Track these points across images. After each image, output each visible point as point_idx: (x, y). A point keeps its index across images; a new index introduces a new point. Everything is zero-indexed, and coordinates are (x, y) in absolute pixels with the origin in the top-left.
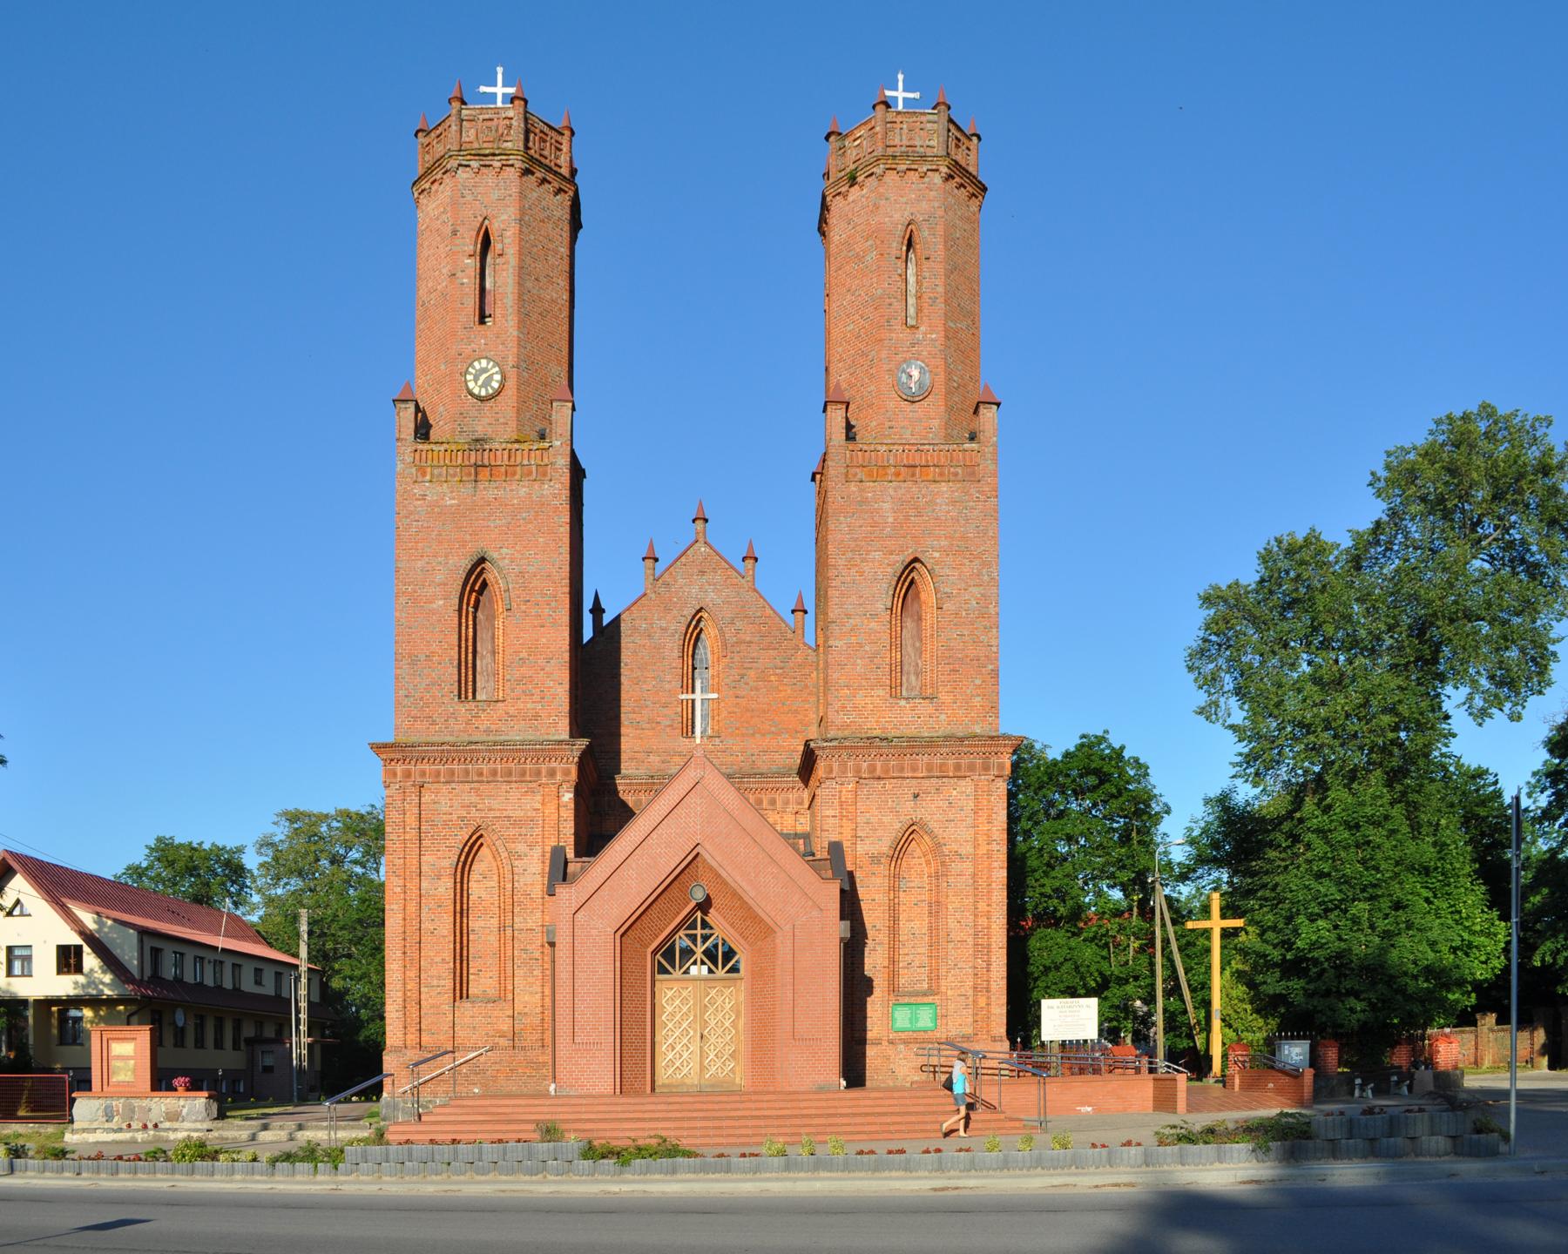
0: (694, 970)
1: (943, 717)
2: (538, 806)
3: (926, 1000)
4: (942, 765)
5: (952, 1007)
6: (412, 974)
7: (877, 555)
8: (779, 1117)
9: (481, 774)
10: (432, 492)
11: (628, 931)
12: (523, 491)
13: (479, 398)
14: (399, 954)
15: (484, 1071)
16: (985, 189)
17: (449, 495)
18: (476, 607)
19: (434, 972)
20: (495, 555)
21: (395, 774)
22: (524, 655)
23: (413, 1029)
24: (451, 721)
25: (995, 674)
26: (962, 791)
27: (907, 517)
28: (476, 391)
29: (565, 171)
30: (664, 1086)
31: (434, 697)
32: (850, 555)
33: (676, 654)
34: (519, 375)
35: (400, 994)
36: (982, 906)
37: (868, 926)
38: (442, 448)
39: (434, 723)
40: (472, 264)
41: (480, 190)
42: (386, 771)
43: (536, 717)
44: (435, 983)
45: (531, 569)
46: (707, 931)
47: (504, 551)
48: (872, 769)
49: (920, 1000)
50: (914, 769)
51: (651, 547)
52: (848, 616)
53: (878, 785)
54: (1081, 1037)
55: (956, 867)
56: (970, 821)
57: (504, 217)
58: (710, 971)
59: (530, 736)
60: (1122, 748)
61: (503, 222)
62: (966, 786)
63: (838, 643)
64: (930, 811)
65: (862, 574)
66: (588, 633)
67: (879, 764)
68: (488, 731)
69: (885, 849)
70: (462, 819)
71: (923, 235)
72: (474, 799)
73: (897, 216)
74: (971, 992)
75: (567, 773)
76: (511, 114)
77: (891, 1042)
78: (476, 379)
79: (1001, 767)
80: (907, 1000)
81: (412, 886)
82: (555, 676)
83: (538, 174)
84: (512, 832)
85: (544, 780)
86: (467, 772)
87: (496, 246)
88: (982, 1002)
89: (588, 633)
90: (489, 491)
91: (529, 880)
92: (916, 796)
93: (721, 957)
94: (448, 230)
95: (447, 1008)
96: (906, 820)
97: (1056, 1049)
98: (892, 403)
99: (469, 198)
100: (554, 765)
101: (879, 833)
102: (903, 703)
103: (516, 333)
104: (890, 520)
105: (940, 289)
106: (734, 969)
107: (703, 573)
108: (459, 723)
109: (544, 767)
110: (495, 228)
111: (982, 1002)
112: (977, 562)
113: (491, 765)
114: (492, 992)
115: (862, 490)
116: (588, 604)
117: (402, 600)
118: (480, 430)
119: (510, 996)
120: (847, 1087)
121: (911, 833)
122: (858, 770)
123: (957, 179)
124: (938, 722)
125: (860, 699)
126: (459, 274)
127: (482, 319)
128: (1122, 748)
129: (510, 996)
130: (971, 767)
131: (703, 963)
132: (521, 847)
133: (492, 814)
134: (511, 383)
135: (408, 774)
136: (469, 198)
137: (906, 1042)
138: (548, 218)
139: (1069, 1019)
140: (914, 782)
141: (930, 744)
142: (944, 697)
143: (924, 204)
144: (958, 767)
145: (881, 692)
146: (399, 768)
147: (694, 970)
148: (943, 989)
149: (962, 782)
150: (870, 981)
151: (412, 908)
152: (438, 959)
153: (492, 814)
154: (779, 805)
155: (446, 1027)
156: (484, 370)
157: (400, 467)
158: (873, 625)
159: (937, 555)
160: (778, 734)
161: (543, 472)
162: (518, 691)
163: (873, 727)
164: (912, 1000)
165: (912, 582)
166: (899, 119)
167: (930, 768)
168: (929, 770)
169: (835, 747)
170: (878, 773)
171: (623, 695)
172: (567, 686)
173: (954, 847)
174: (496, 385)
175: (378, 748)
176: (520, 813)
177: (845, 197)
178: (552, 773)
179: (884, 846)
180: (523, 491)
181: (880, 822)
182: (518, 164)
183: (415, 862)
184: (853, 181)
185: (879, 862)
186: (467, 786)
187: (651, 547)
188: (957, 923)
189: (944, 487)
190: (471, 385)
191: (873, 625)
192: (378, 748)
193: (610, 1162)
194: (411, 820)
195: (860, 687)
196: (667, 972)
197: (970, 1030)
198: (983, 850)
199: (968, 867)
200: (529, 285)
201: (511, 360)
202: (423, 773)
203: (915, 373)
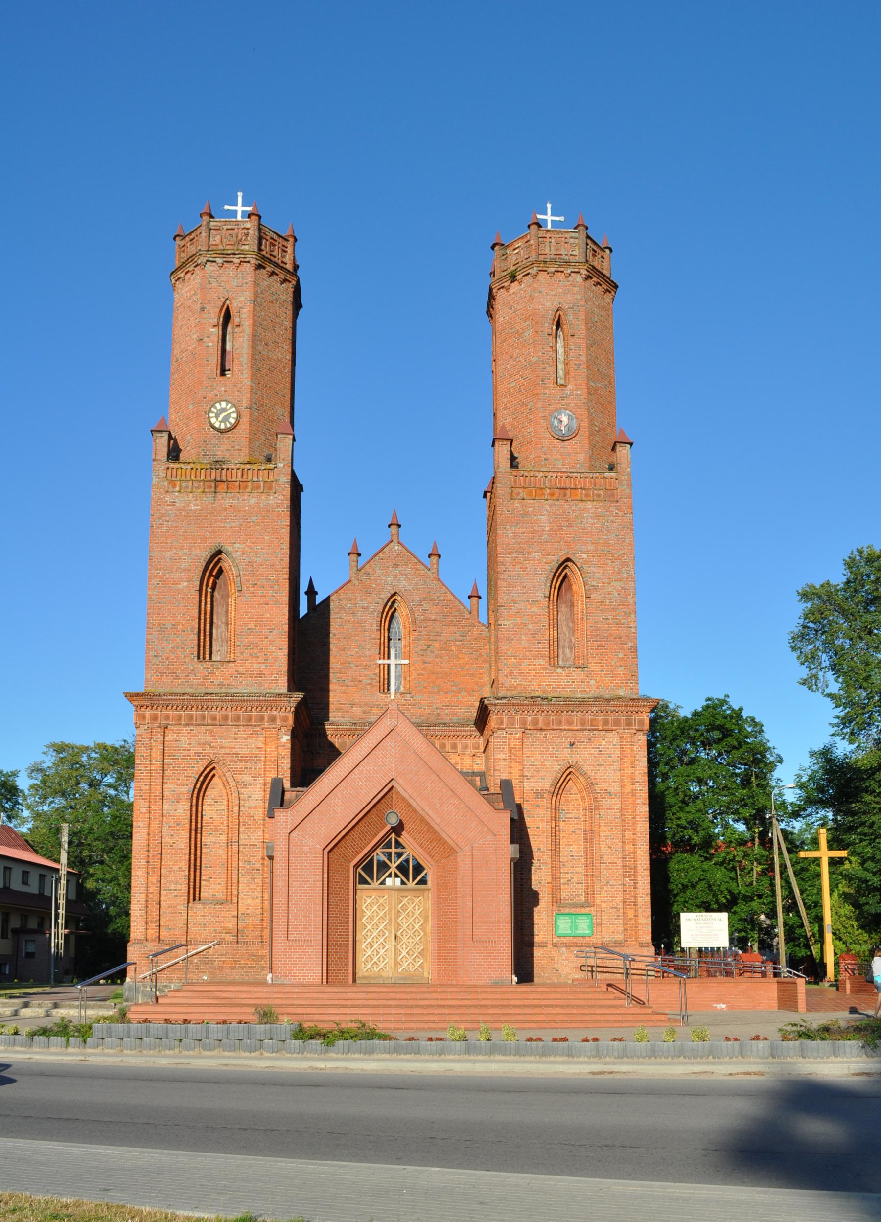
0: (389, 882)
1: (593, 682)
2: (261, 745)
3: (583, 911)
4: (592, 720)
5: (605, 917)
6: (154, 879)
7: (537, 555)
8: (461, 1006)
9: (215, 719)
10: (180, 500)
11: (333, 848)
12: (253, 501)
13: (219, 430)
14: (143, 862)
15: (212, 962)
16: (616, 287)
17: (195, 502)
18: (214, 588)
19: (172, 878)
20: (230, 549)
21: (144, 718)
22: (251, 626)
23: (153, 925)
24: (192, 677)
25: (634, 650)
26: (610, 741)
27: (560, 527)
28: (217, 425)
29: (289, 267)
30: (364, 978)
31: (178, 657)
32: (515, 555)
33: (375, 627)
34: (251, 415)
35: (143, 896)
36: (628, 834)
37: (534, 848)
38: (189, 467)
39: (177, 678)
40: (216, 332)
41: (223, 279)
42: (137, 715)
43: (261, 675)
44: (173, 887)
45: (259, 560)
46: (399, 850)
47: (237, 545)
48: (535, 722)
49: (578, 910)
50: (570, 723)
51: (355, 545)
53: (540, 735)
54: (715, 945)
55: (606, 802)
56: (616, 765)
57: (242, 299)
58: (403, 883)
59: (255, 689)
60: (741, 709)
61: (241, 302)
62: (613, 738)
63: (507, 623)
64: (584, 757)
65: (524, 569)
66: (303, 610)
67: (541, 719)
68: (221, 685)
69: (547, 787)
70: (198, 754)
71: (569, 319)
72: (209, 738)
73: (548, 304)
74: (621, 906)
75: (285, 719)
76: (248, 225)
77: (555, 945)
78: (217, 417)
79: (641, 722)
80: (567, 910)
81: (156, 807)
82: (276, 643)
83: (269, 269)
84: (240, 765)
85: (266, 725)
86: (203, 717)
87: (235, 319)
88: (631, 914)
89: (303, 610)
90: (226, 500)
91: (253, 805)
92: (572, 745)
93: (412, 871)
94: (198, 307)
95: (182, 908)
96: (564, 763)
97: (694, 955)
98: (547, 441)
99: (215, 284)
100: (274, 713)
101: (542, 773)
102: (559, 670)
103: (249, 383)
104: (547, 529)
105: (583, 358)
106: (423, 882)
107: (396, 565)
108: (195, 677)
109: (266, 715)
110: (234, 307)
111: (631, 914)
112: (617, 562)
113: (223, 712)
114: (220, 896)
115: (523, 506)
116: (304, 587)
117: (154, 581)
118: (220, 454)
119: (235, 899)
120: (518, 983)
121: (568, 774)
122: (524, 723)
123: (595, 279)
124: (588, 686)
125: (525, 666)
126: (206, 339)
127: (223, 372)
128: (741, 709)
129: (235, 899)
130: (617, 723)
131: (396, 876)
132: (246, 778)
133: (223, 751)
134: (245, 420)
135: (155, 718)
136: (215, 284)
137: (568, 946)
138: (276, 300)
139: (704, 930)
140: (570, 733)
141: (583, 703)
142: (593, 666)
144: (606, 722)
145: (542, 662)
146: (148, 713)
147: (389, 882)
148: (598, 902)
149: (610, 735)
150: (536, 894)
151: (155, 825)
152: (176, 868)
153: (223, 751)
154: (459, 748)
155: (181, 924)
156: (224, 410)
157: (155, 480)
158: (534, 609)
159: (585, 556)
160: (459, 692)
161: (269, 487)
162: (247, 653)
163: (536, 688)
164: (572, 910)
165: (565, 576)
166: (548, 235)
167: (583, 722)
168: (582, 724)
169: (505, 704)
170: (541, 725)
171: (332, 659)
172: (286, 651)
173: (604, 786)
174: (233, 421)
175: (131, 696)
176: (245, 751)
177: (507, 289)
178: (273, 719)
179: (546, 784)
180: (253, 501)
181: (543, 765)
182: (253, 261)
183: (159, 788)
184: (513, 278)
185: (542, 797)
186: (203, 728)
187: (355, 545)
188: (608, 847)
189: (589, 505)
190: (213, 420)
191: (534, 609)
192: (131, 696)
193: (317, 1043)
194: (157, 755)
196: (367, 883)
197: (621, 937)
198: (628, 789)
199: (616, 802)
200: (260, 348)
201: (245, 403)
202: (167, 717)
203: (565, 419)
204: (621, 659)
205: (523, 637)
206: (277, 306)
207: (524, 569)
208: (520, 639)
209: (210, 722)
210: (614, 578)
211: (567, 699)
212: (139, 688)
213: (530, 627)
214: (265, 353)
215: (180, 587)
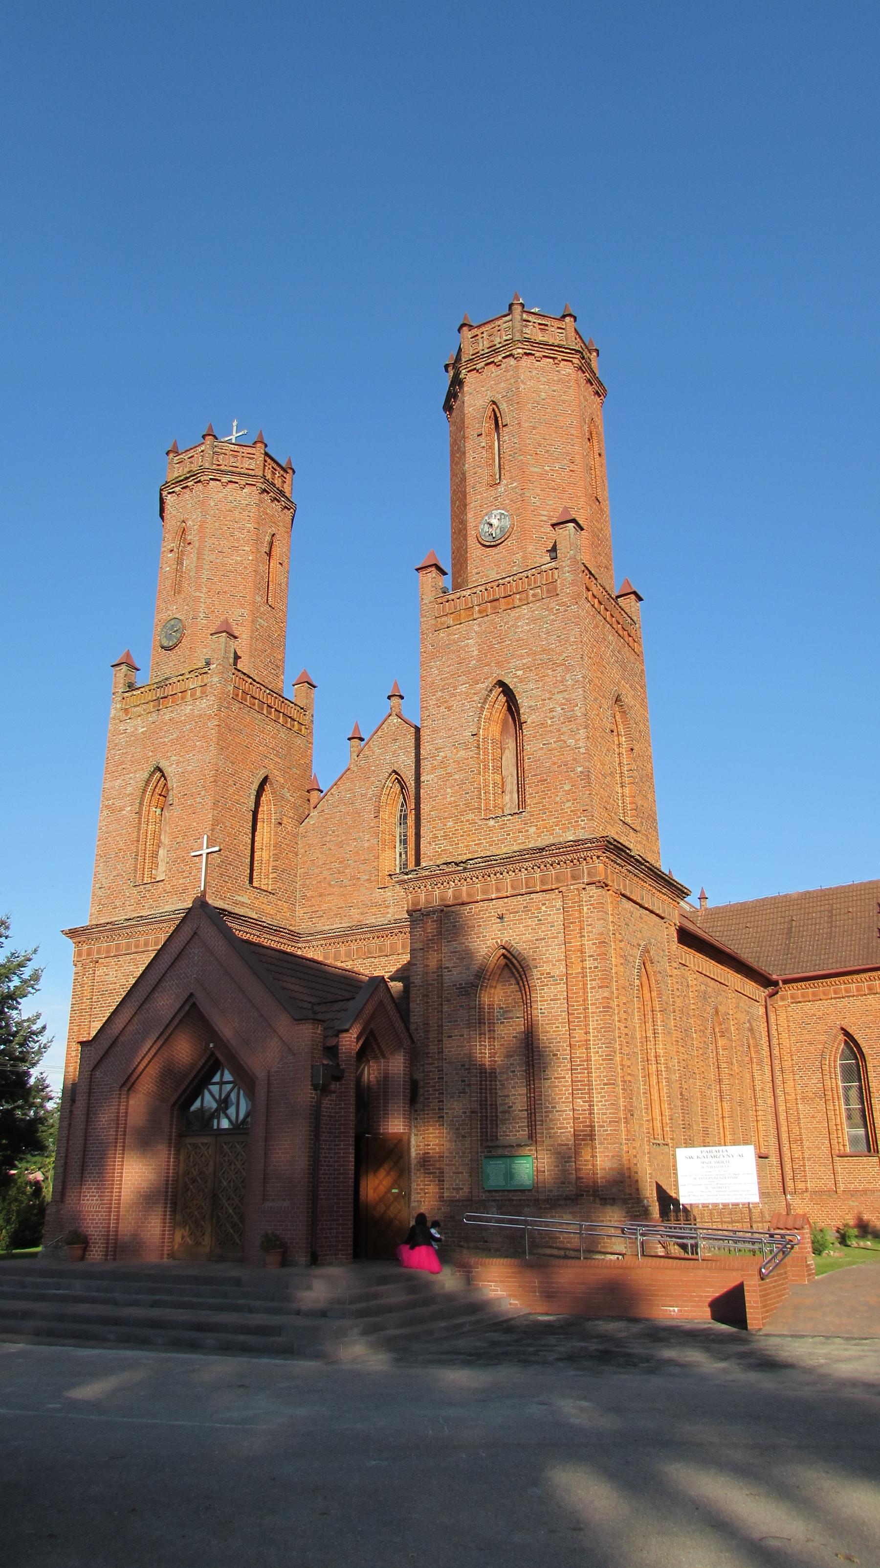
1: (533, 830)
63: (429, 777)
83: (224, 480)
92: (501, 918)
135: (89, 953)
140: (500, 902)
143: (503, 385)
146: (85, 947)
157: (113, 712)
159: (520, 673)
175: (72, 933)
189: (525, 610)
192: (72, 933)
198: (576, 969)
204: (567, 793)
206: (237, 513)
207: (449, 708)
210: (557, 690)
211: (486, 859)
212: (84, 922)
213: (457, 777)
214: (218, 561)
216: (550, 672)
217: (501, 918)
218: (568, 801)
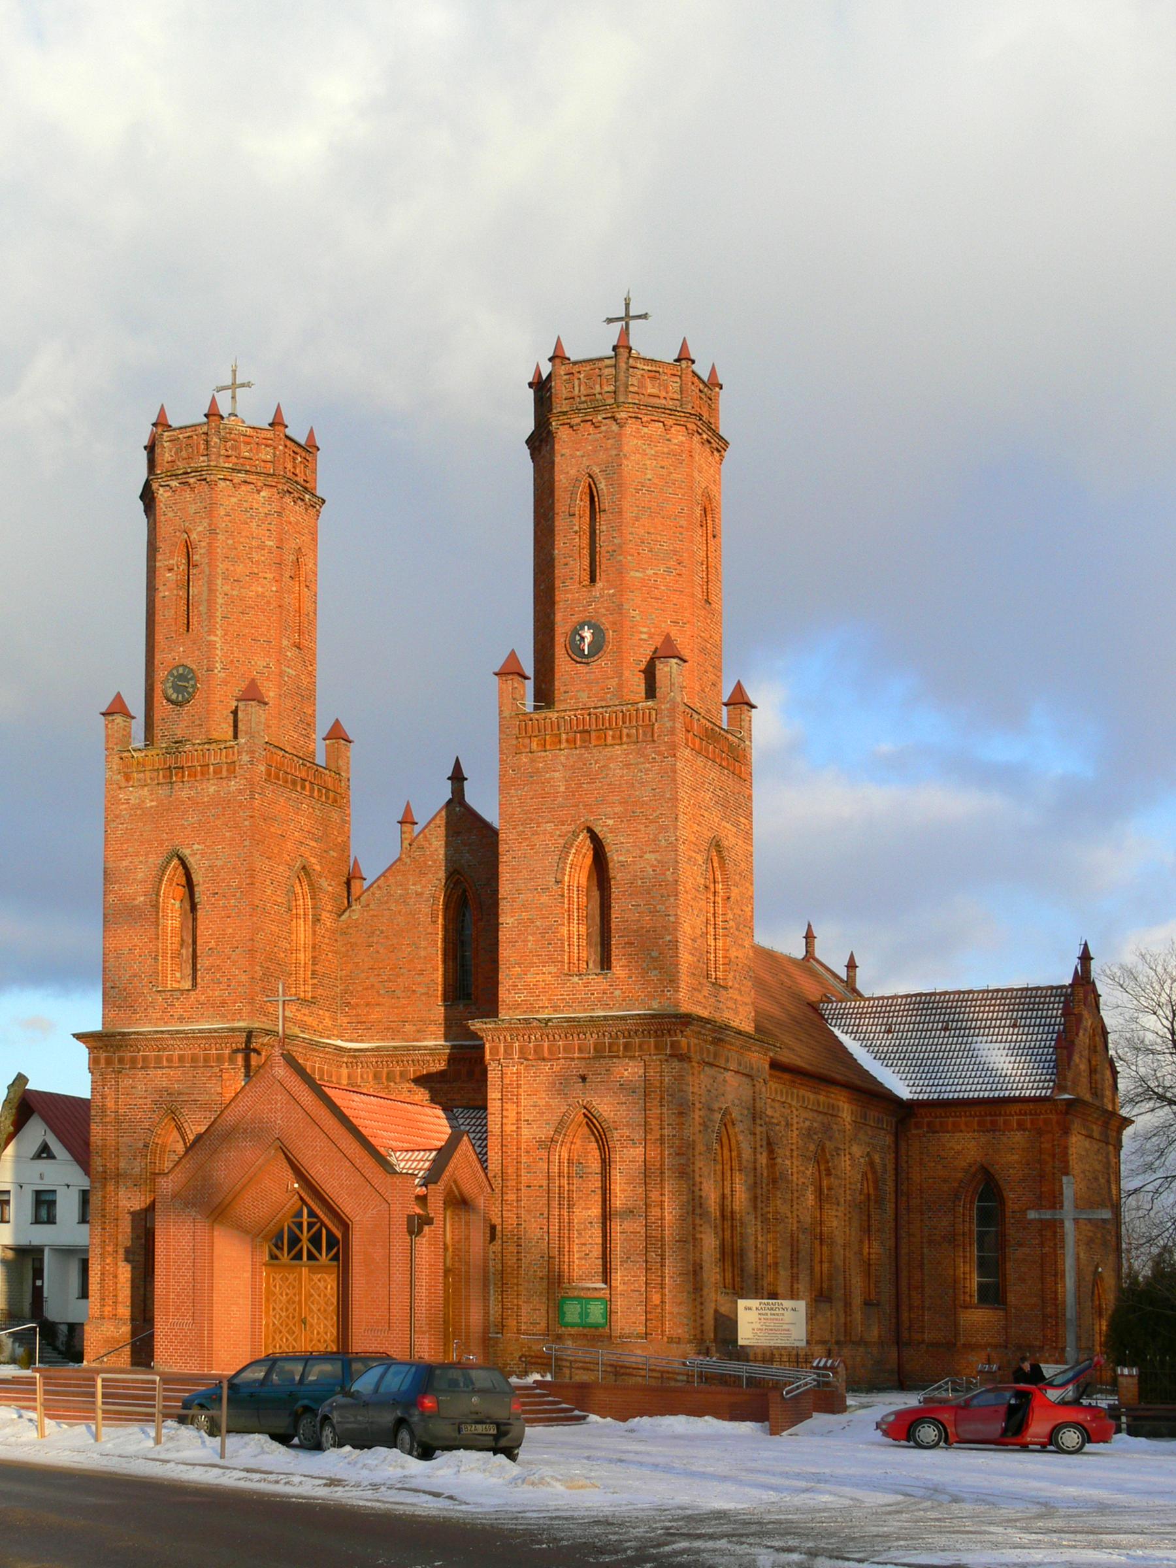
1: (617, 993)
7: (549, 827)
12: (212, 790)
24: (150, 1010)
27: (580, 785)
32: (521, 828)
45: (219, 863)
47: (196, 847)
48: (538, 1049)
52: (519, 892)
57: (200, 529)
61: (199, 533)
65: (533, 847)
90: (184, 793)
99: (171, 515)
104: (562, 789)
112: (653, 826)
115: (532, 761)
125: (531, 978)
138: (252, 517)
145: (553, 969)
159: (610, 822)
189: (618, 750)
191: (545, 899)
195: (532, 965)
205: (530, 938)
207: (533, 847)
208: (526, 941)
209: (165, 1064)
210: (649, 849)
212: (96, 1026)
213: (538, 923)
214: (235, 593)
215: (137, 902)
216: (642, 827)
217: (584, 1079)
218: (655, 969)
